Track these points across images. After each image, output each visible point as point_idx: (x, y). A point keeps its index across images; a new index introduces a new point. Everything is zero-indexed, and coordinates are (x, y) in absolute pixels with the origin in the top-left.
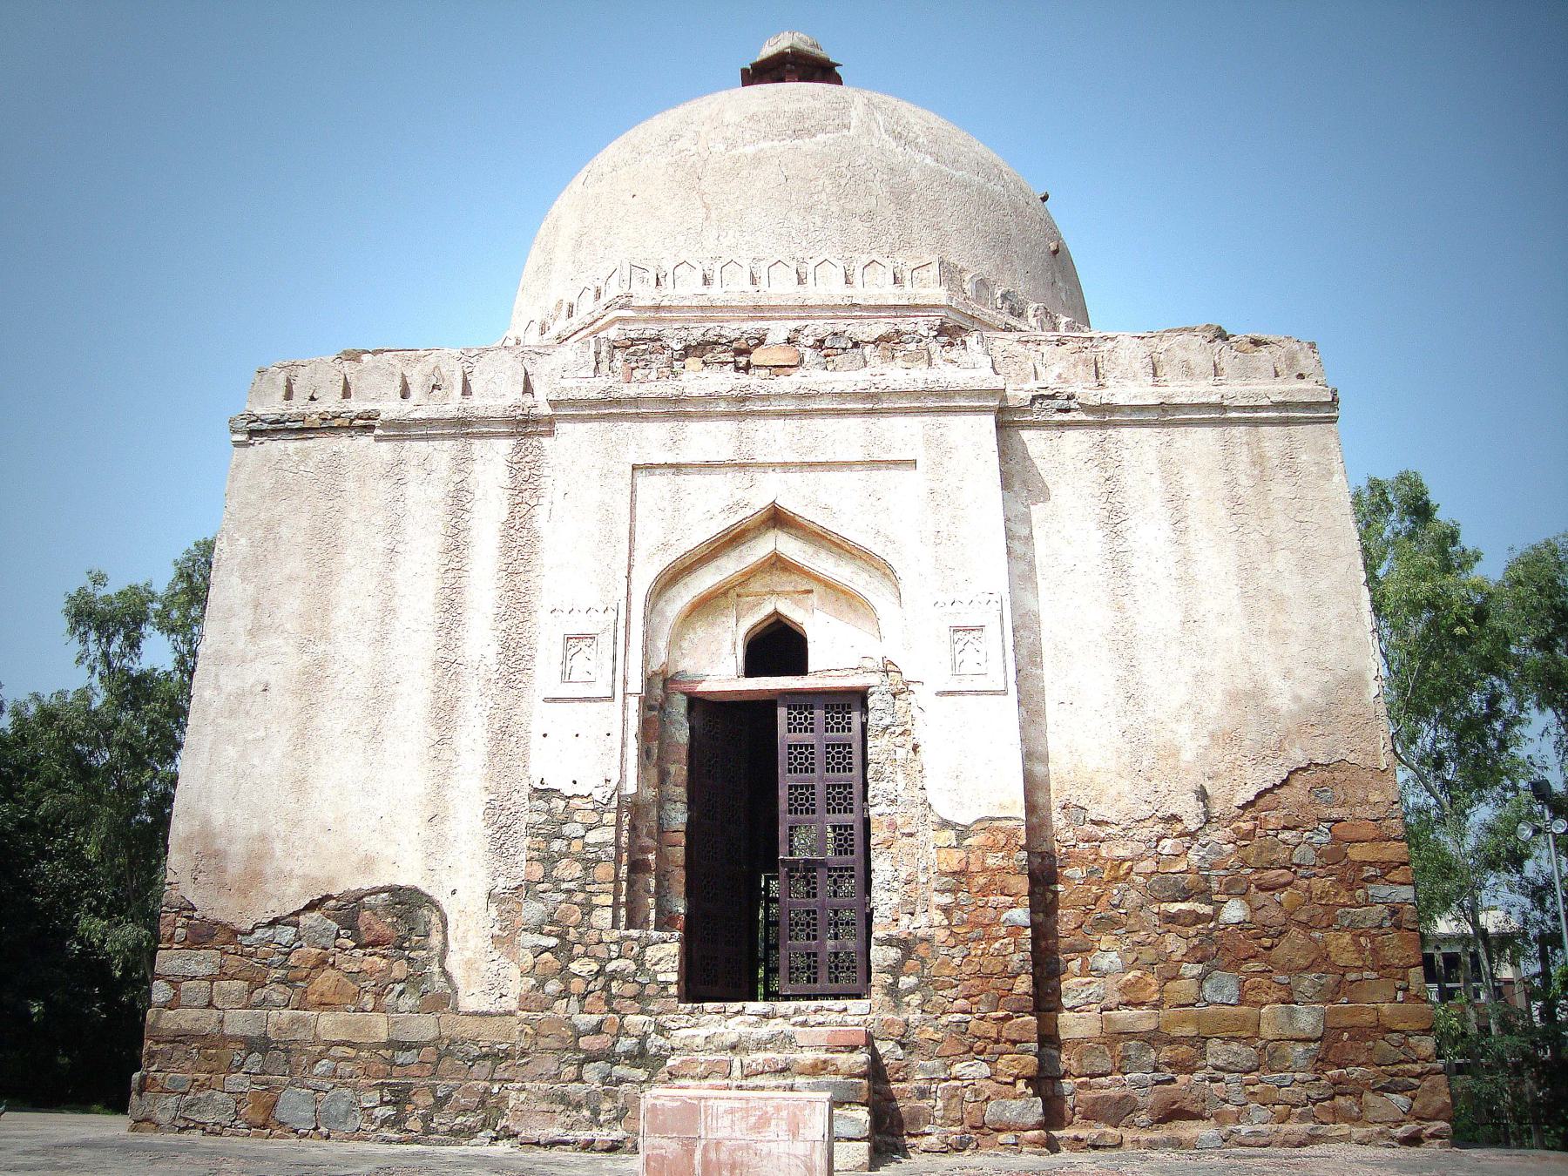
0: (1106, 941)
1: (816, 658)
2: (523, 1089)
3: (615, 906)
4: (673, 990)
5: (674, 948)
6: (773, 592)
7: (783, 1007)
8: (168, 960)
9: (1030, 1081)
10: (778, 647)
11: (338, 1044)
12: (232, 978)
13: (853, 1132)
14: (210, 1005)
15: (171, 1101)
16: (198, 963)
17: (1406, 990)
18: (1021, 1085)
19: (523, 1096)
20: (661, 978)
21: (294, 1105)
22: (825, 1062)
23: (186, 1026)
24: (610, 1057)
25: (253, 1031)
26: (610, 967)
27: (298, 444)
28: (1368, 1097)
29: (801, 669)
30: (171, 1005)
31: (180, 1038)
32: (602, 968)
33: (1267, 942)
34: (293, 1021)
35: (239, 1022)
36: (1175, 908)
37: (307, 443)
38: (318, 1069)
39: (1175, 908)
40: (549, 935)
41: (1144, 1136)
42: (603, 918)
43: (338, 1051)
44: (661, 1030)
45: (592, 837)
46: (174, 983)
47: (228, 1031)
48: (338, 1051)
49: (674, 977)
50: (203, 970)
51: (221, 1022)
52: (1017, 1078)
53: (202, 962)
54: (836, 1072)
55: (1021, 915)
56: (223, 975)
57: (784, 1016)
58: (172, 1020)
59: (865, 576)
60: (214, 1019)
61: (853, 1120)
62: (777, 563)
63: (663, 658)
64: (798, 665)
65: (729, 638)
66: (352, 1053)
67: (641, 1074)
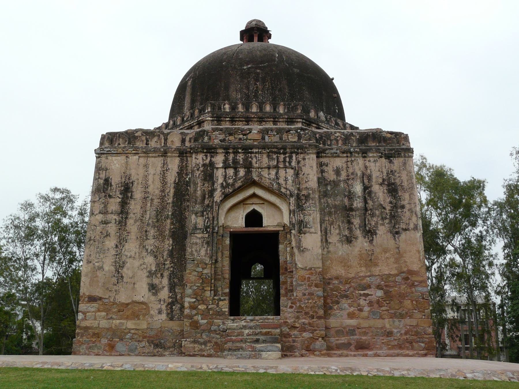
0: (344, 301)
1: (265, 223)
2: (186, 341)
3: (211, 290)
4: (227, 313)
5: (227, 302)
6: (253, 204)
7: (257, 318)
8: (82, 307)
9: (323, 338)
10: (254, 218)
11: (133, 329)
12: (102, 311)
13: (276, 349)
14: (95, 319)
15: (84, 347)
16: (91, 308)
17: (424, 315)
18: (320, 339)
19: (186, 342)
20: (223, 310)
21: (120, 346)
22: (269, 332)
23: (88, 325)
24: (210, 331)
25: (107, 326)
26: (210, 307)
27: (116, 158)
28: (414, 344)
29: (261, 225)
30: (85, 319)
31: (86, 328)
32: (208, 307)
33: (388, 302)
34: (120, 323)
35: (104, 324)
36: (362, 292)
37: (118, 158)
38: (127, 337)
39: (362, 292)
40: (193, 298)
41: (353, 353)
42: (208, 294)
43: (133, 331)
44: (224, 323)
45: (205, 271)
46: (84, 313)
47: (101, 326)
48: (133, 331)
49: (227, 310)
50: (93, 310)
51: (99, 324)
52: (319, 337)
53: (92, 307)
54: (272, 335)
55: (321, 293)
56: (99, 311)
57: (257, 320)
58: (84, 324)
59: (279, 200)
60: (97, 323)
61: (277, 347)
62: (254, 195)
63: (223, 222)
64: (260, 224)
65: (241, 216)
66: (137, 332)
67: (218, 336)
